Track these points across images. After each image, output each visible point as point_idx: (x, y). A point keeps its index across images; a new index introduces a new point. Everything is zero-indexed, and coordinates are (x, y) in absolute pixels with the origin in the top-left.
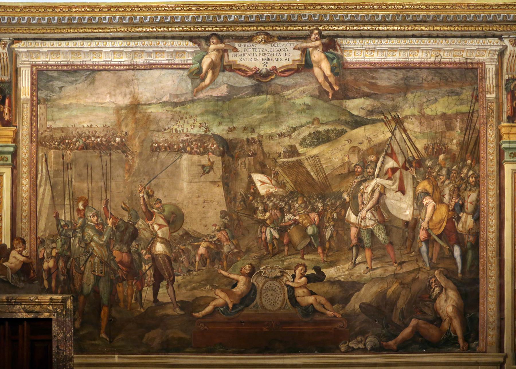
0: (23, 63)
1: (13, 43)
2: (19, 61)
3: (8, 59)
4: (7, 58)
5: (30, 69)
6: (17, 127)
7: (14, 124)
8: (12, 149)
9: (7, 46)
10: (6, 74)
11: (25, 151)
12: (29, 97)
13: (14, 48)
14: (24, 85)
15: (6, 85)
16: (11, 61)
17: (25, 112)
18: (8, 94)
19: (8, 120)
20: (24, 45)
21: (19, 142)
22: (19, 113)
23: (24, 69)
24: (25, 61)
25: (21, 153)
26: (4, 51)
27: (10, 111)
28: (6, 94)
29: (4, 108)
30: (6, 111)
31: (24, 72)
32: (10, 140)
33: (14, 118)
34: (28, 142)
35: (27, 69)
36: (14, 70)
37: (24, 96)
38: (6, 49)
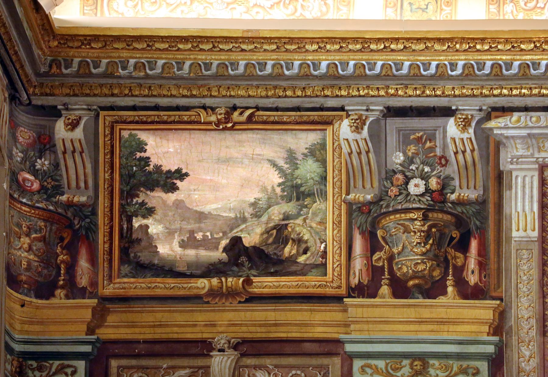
0: (516, 160)
1: (488, 117)
2: (505, 156)
3: (476, 153)
4: (473, 151)
5: (536, 174)
6: (501, 299)
7: (494, 294)
8: (491, 349)
9: (473, 124)
10: (472, 184)
11: (527, 353)
12: (536, 234)
13: (491, 129)
14: (520, 209)
15: (471, 210)
16: (485, 157)
17: (525, 267)
18: (477, 228)
19: (476, 284)
20: (519, 121)
21: (509, 332)
22: (509, 270)
23: (521, 174)
24: (522, 157)
25: (516, 356)
26: (465, 136)
27: (482, 265)
28: (472, 227)
29: (466, 258)
30: (472, 264)
31: (520, 180)
32: (486, 328)
33: (493, 281)
34: (533, 333)
35: (530, 174)
36: (492, 175)
37: (521, 233)
38: (471, 131)
